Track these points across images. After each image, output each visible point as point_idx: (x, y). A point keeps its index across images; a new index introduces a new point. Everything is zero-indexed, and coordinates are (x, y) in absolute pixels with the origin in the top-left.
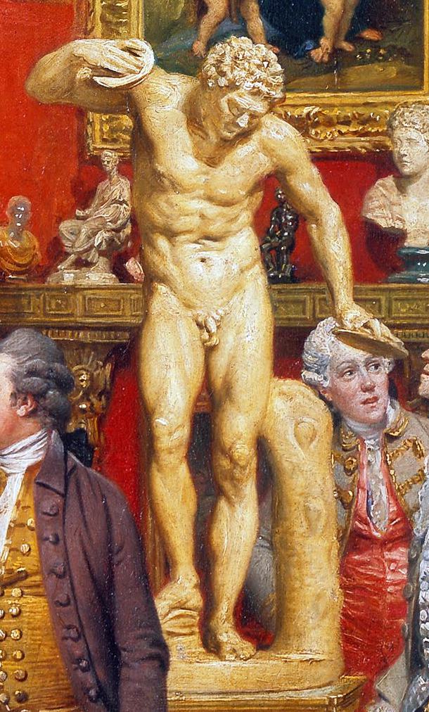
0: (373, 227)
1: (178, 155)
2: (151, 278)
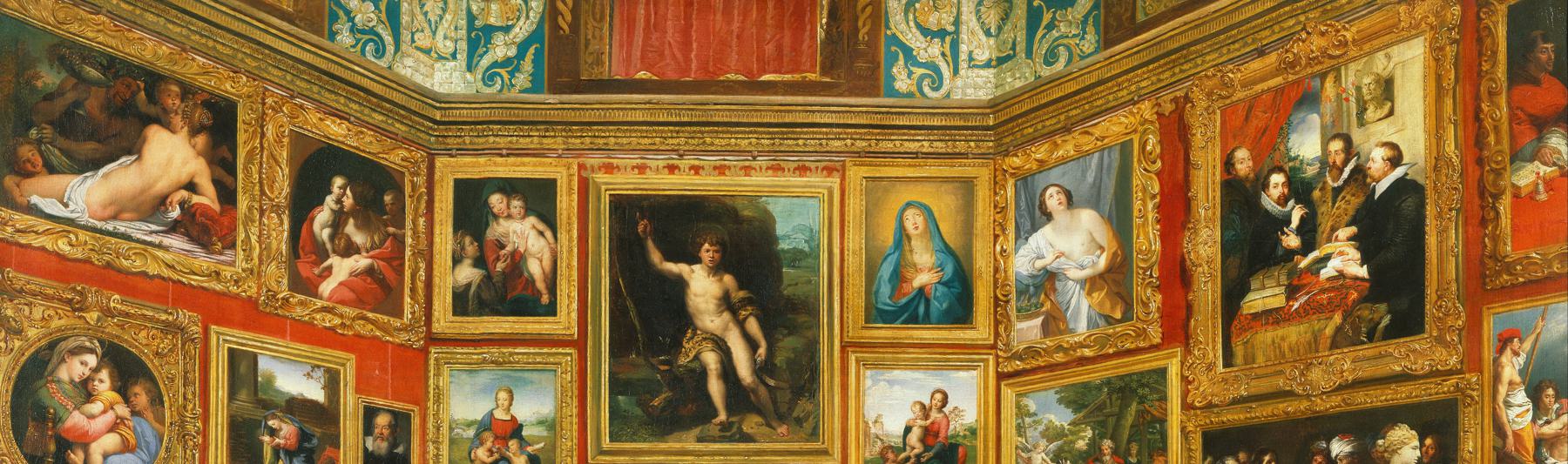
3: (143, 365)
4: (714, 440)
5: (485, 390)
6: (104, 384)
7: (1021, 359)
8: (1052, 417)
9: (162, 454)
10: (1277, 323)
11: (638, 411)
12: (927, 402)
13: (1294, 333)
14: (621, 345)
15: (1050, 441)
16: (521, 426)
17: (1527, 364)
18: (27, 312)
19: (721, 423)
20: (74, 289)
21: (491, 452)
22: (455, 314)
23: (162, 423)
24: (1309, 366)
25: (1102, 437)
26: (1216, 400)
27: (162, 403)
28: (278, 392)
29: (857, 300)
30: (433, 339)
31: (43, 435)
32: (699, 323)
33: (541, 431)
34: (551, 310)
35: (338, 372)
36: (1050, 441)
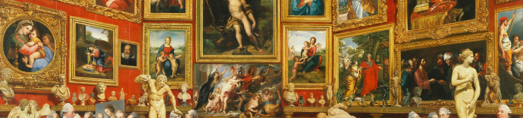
0: (179, 99)
1: (154, 89)
2: (150, 105)
3: (48, 29)
4: (238, 54)
5: (162, 37)
6: (34, 36)
7: (340, 27)
8: (351, 46)
9: (54, 59)
10: (426, 15)
11: (213, 44)
12: (309, 41)
13: (432, 19)
14: (206, 23)
15: (350, 54)
16: (174, 49)
17: (509, 29)
18: (9, 11)
19: (240, 49)
20: (24, 4)
21: (163, 58)
22: (152, 12)
23: (54, 48)
24: (436, 30)
25: (368, 53)
26: (405, 41)
27: (54, 42)
28: (92, 38)
29: (285, 7)
30: (144, 21)
31: (14, 52)
32: (233, 15)
33: (180, 51)
34: (184, 11)
35: (112, 32)
36: (350, 54)
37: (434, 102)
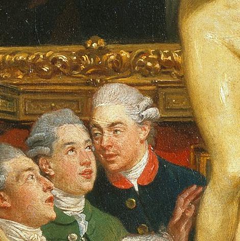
37: (63, 54)
